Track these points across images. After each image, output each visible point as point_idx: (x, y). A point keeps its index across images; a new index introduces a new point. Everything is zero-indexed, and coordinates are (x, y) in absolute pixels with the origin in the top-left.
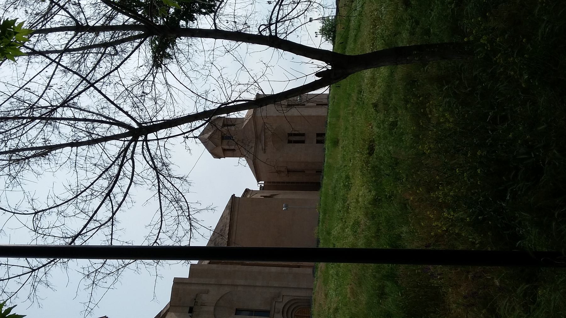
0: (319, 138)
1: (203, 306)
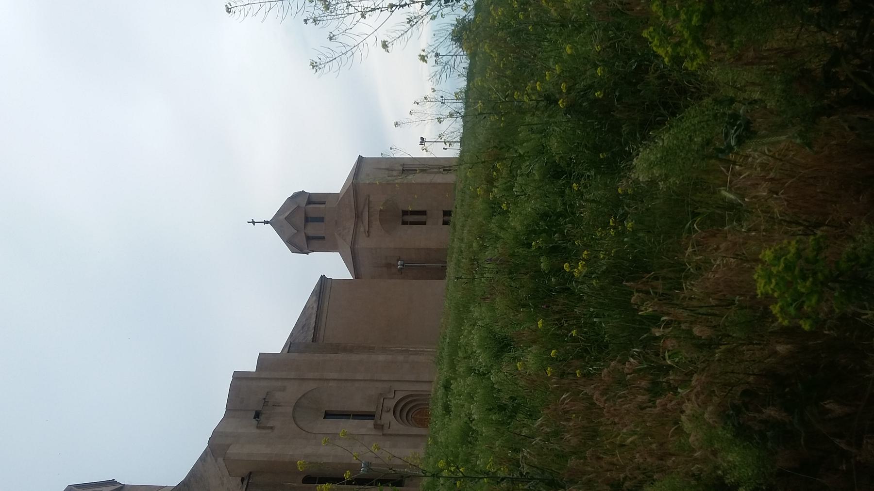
0: (446, 218)
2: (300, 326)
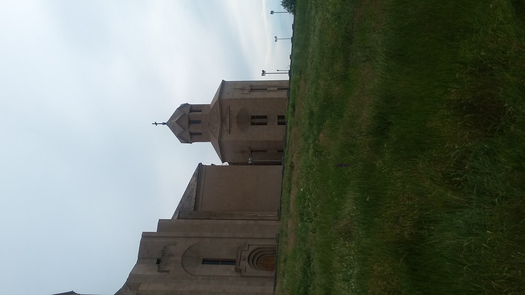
0: (281, 120)
1: (170, 256)
2: (186, 196)
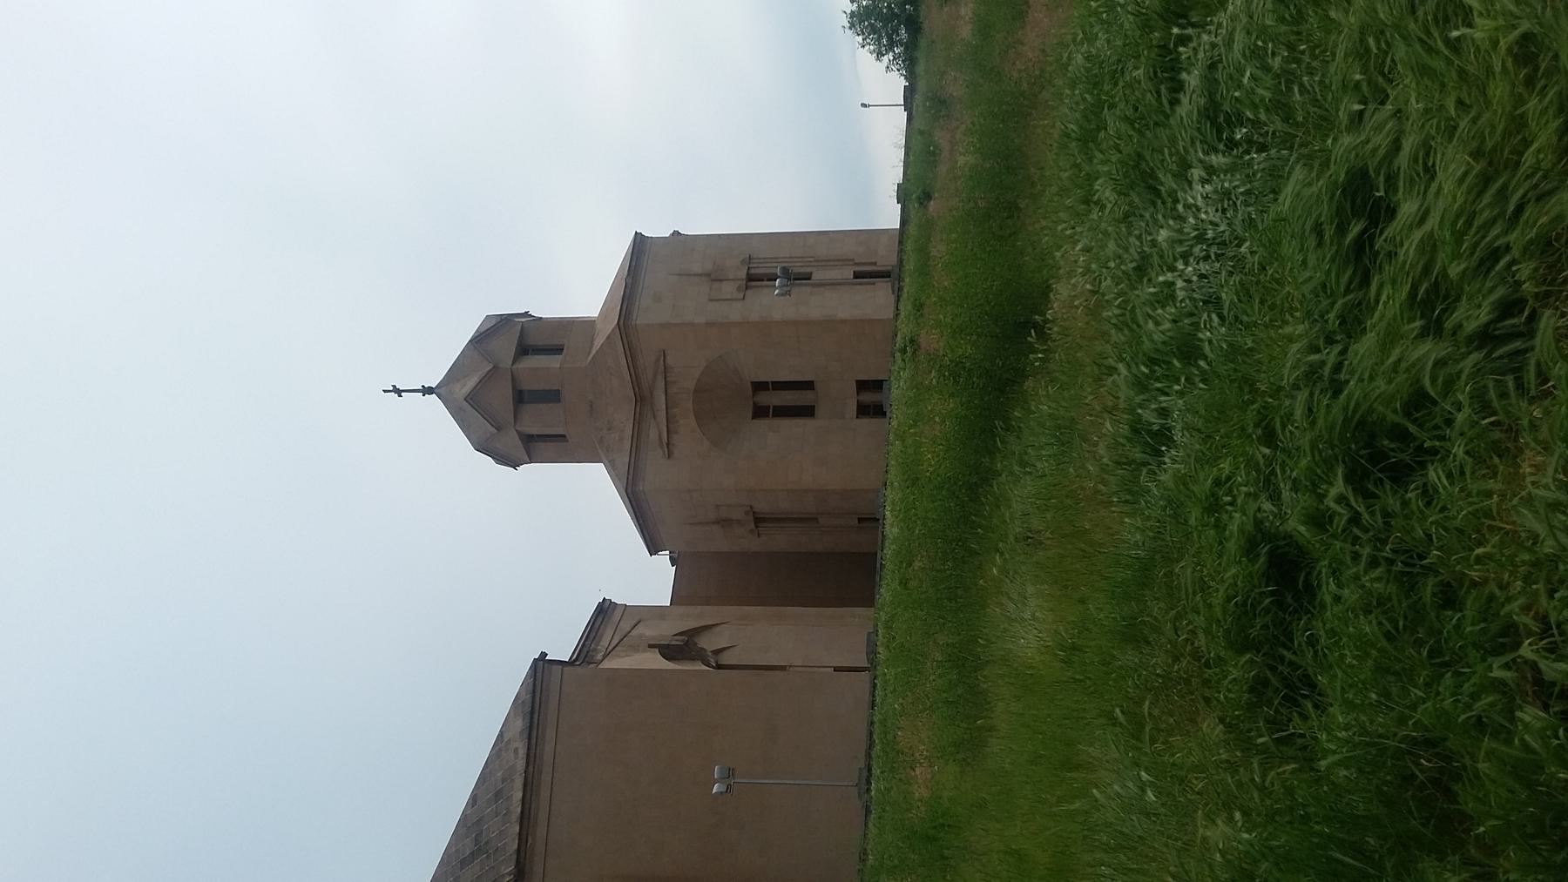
0: (869, 397)
